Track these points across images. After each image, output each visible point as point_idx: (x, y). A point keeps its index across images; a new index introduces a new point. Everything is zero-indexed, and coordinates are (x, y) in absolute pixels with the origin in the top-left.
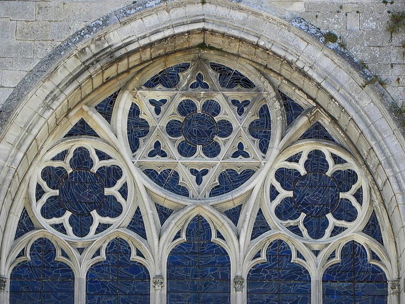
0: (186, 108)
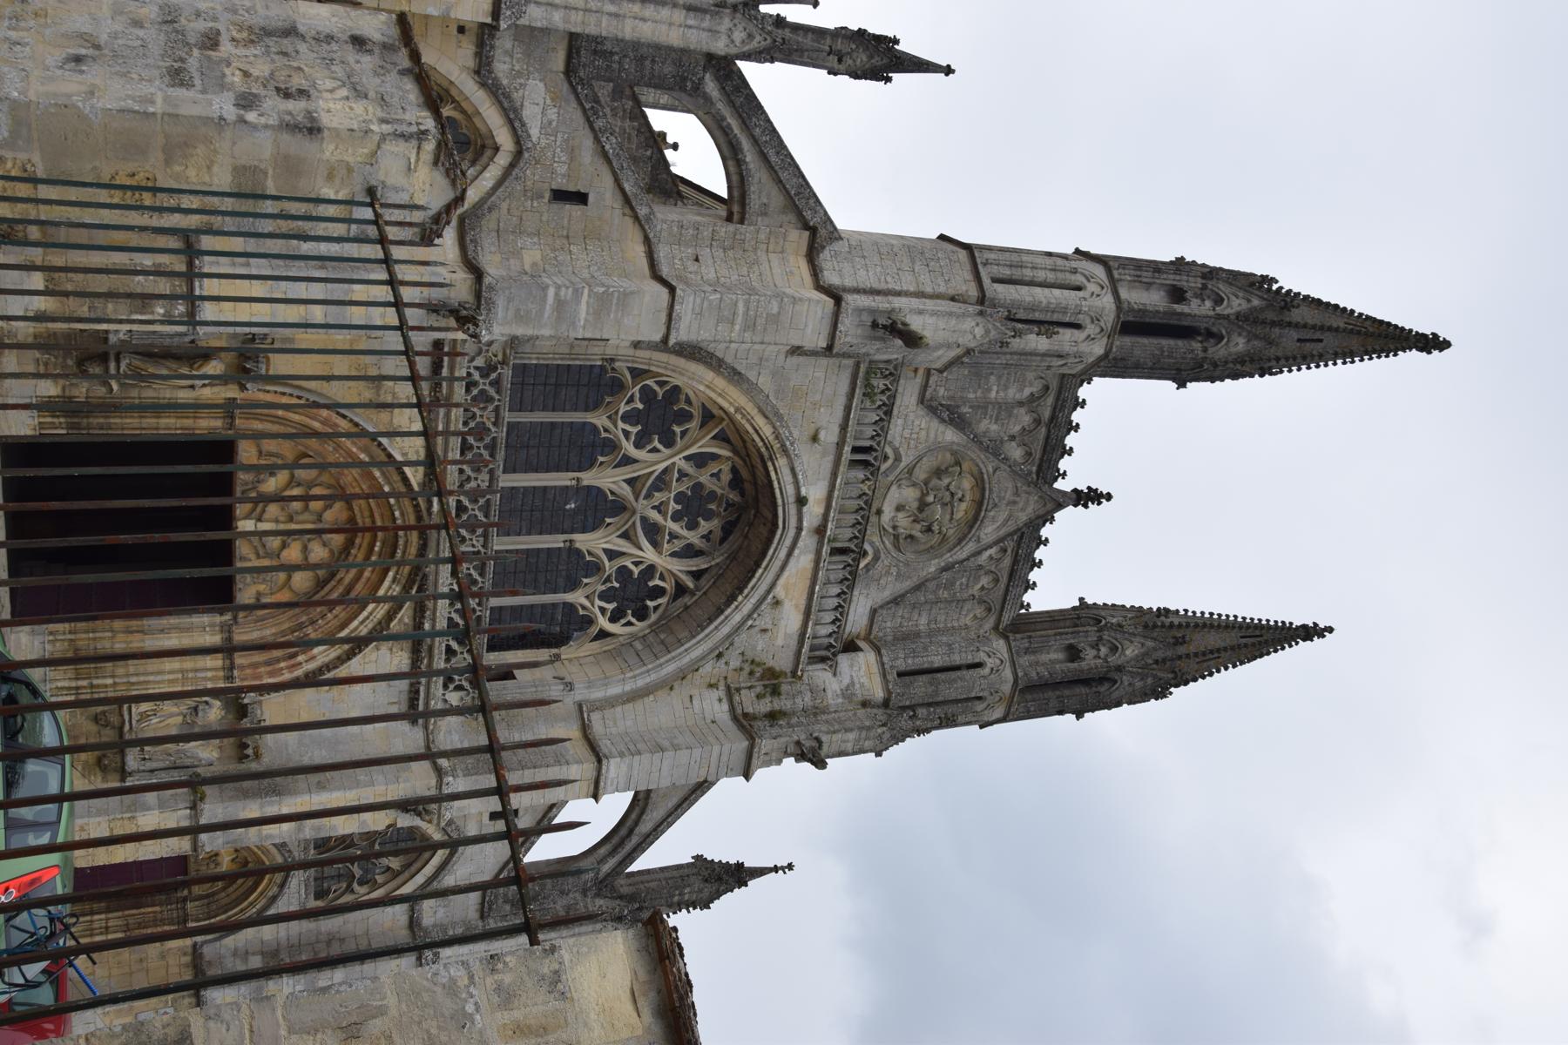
0: (712, 496)
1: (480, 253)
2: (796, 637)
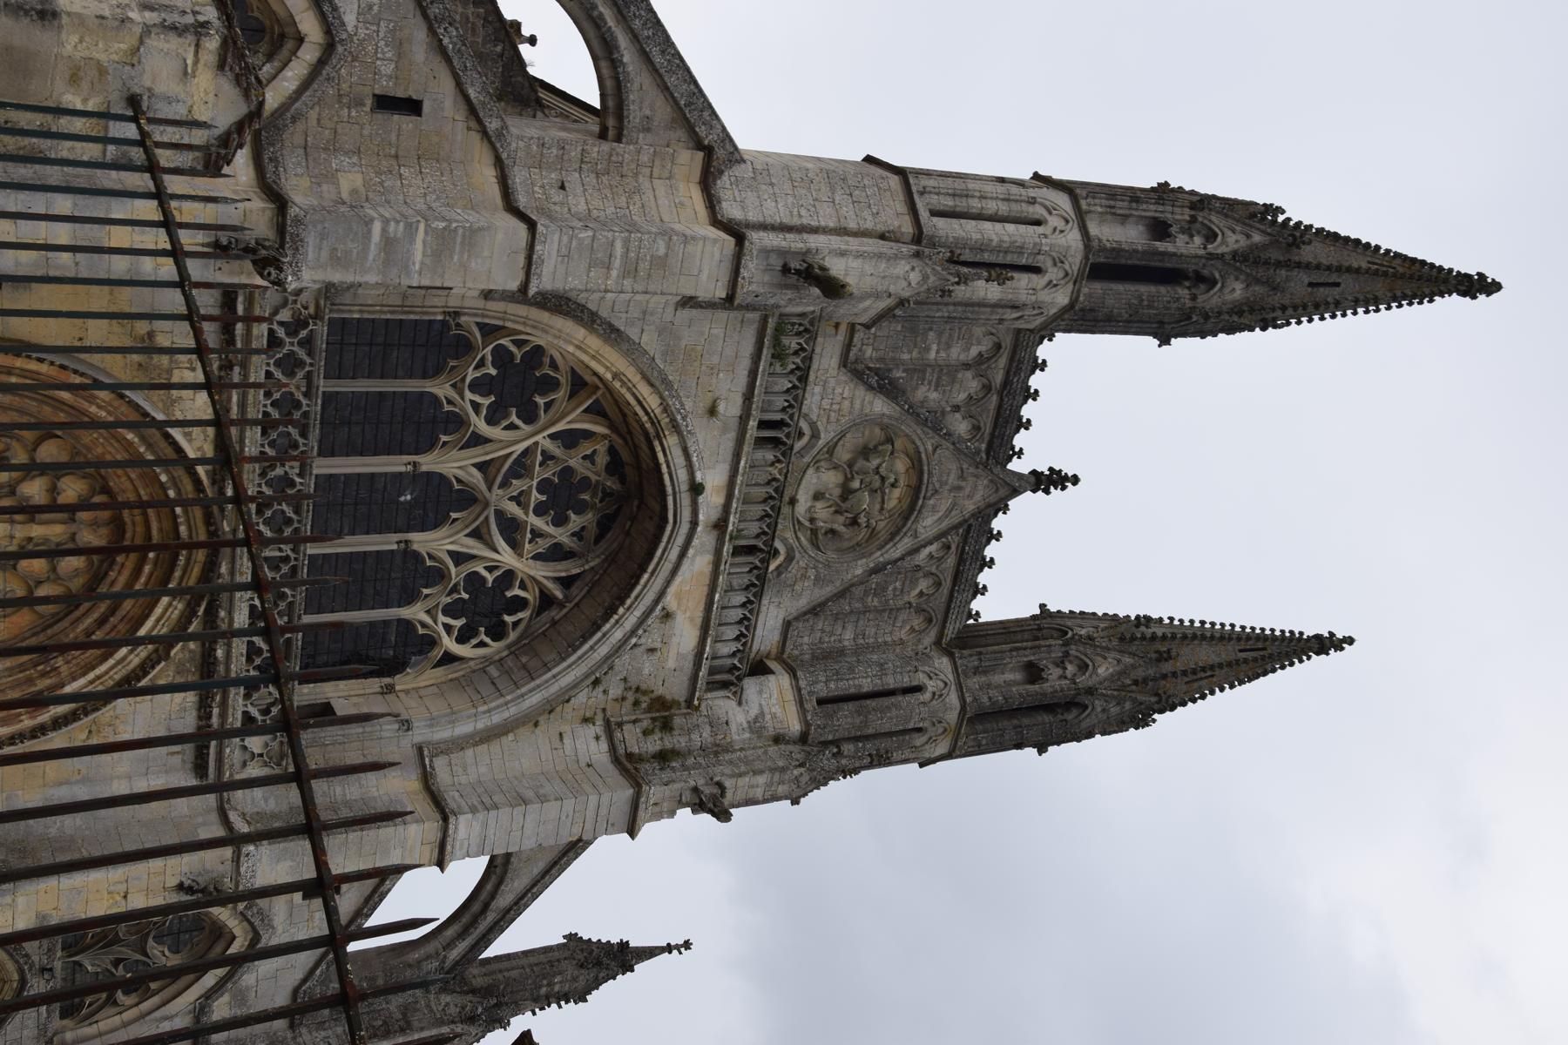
0: (585, 483)
1: (282, 177)
2: (691, 658)
